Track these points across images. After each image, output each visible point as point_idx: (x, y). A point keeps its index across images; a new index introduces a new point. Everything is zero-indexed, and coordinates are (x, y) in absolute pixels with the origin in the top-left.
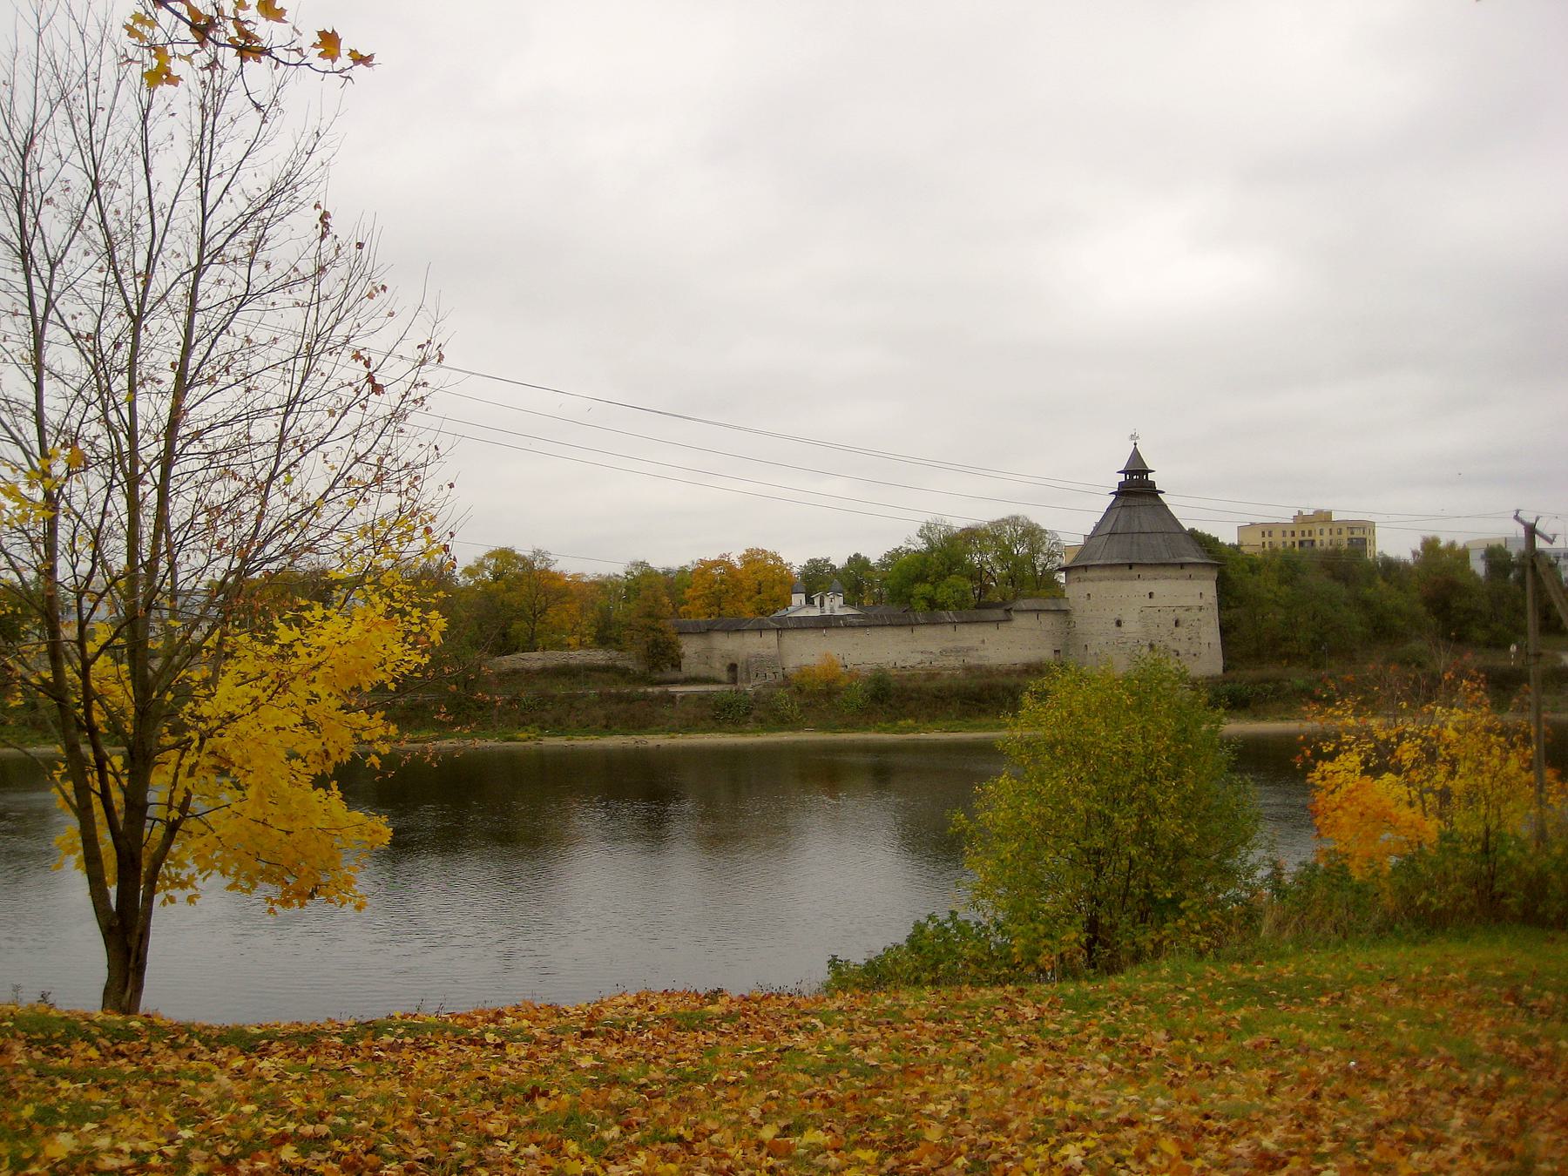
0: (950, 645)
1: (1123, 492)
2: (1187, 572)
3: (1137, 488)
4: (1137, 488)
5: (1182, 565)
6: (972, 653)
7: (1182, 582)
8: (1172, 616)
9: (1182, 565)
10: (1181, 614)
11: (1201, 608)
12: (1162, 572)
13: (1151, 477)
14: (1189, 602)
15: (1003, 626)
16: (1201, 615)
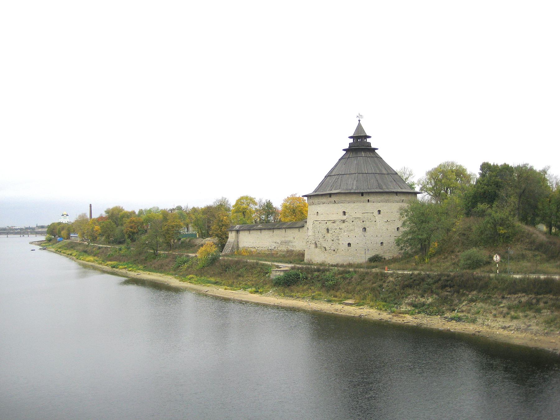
0: (283, 239)
1: (352, 150)
2: (333, 199)
3: (360, 146)
4: (360, 146)
5: (330, 195)
6: (291, 244)
7: (331, 205)
8: (325, 226)
9: (330, 195)
10: (330, 225)
11: (344, 221)
12: (348, 198)
13: (368, 140)
14: (334, 217)
16: (343, 226)
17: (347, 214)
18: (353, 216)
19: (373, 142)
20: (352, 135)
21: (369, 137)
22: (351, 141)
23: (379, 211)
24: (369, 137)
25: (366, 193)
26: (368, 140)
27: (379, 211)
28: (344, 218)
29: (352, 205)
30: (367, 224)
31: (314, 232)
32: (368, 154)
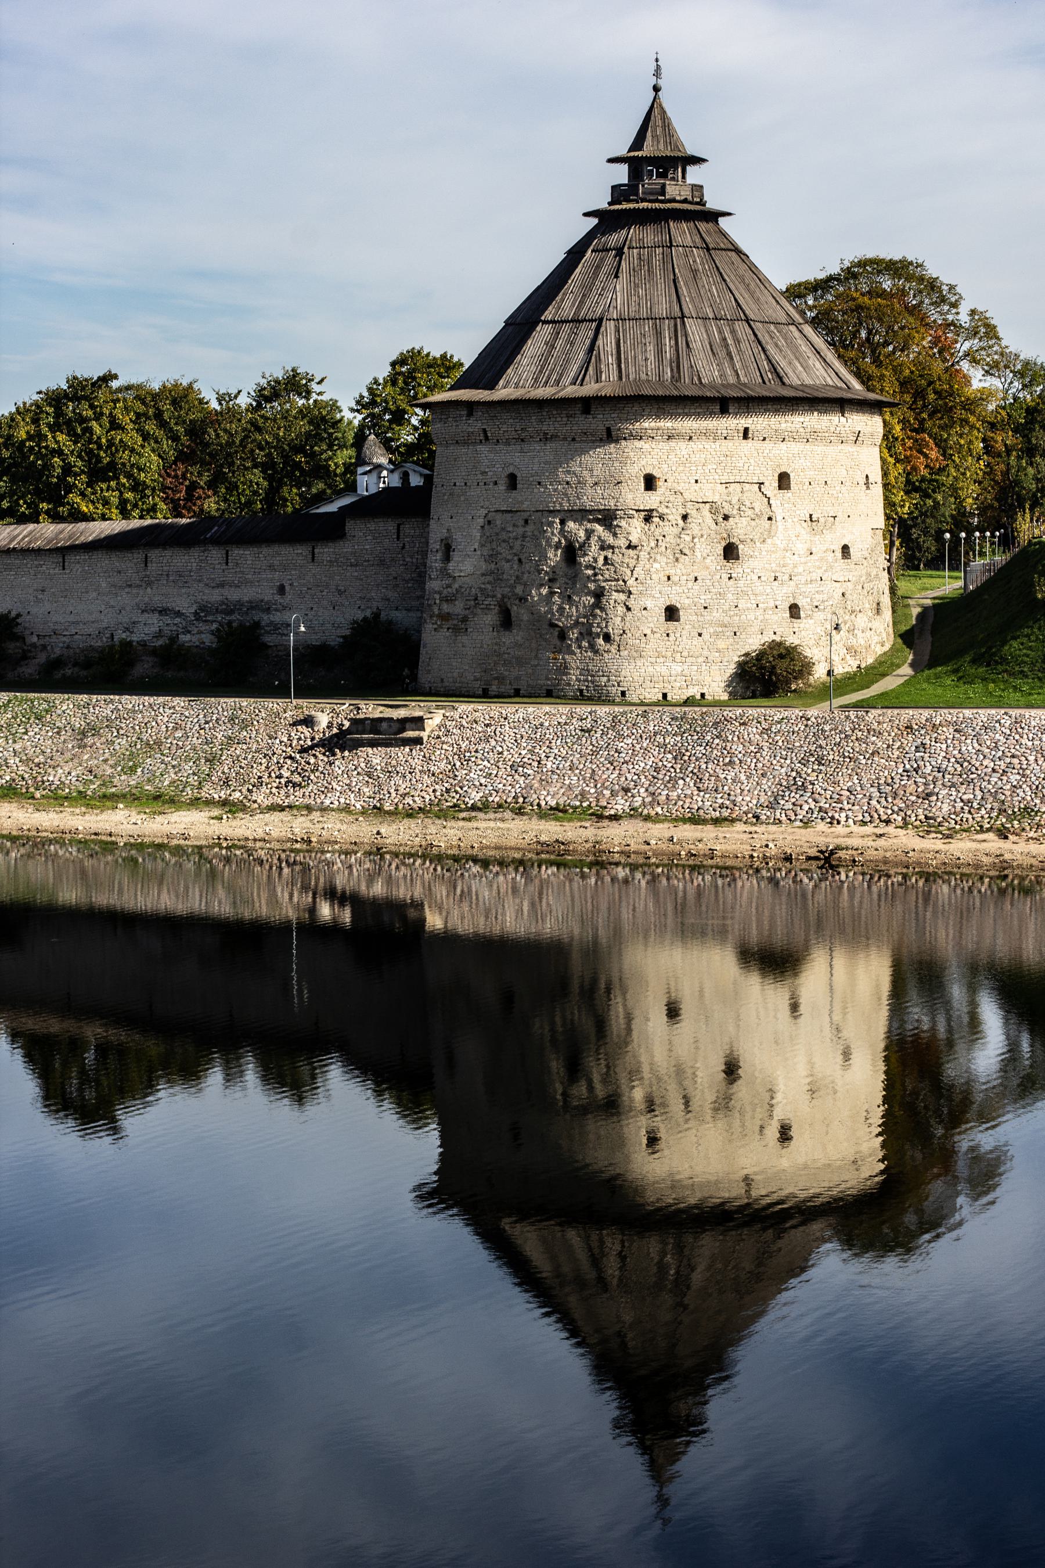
0: (215, 596)
15: (326, 551)
17: (660, 483)
18: (688, 496)
19: (712, 184)
20: (623, 151)
21: (696, 160)
22: (621, 174)
23: (784, 481)
24: (696, 160)
25: (738, 400)
26: (694, 175)
27: (784, 481)
28: (651, 500)
29: (681, 447)
30: (740, 528)
31: (492, 558)
32: (682, 233)
